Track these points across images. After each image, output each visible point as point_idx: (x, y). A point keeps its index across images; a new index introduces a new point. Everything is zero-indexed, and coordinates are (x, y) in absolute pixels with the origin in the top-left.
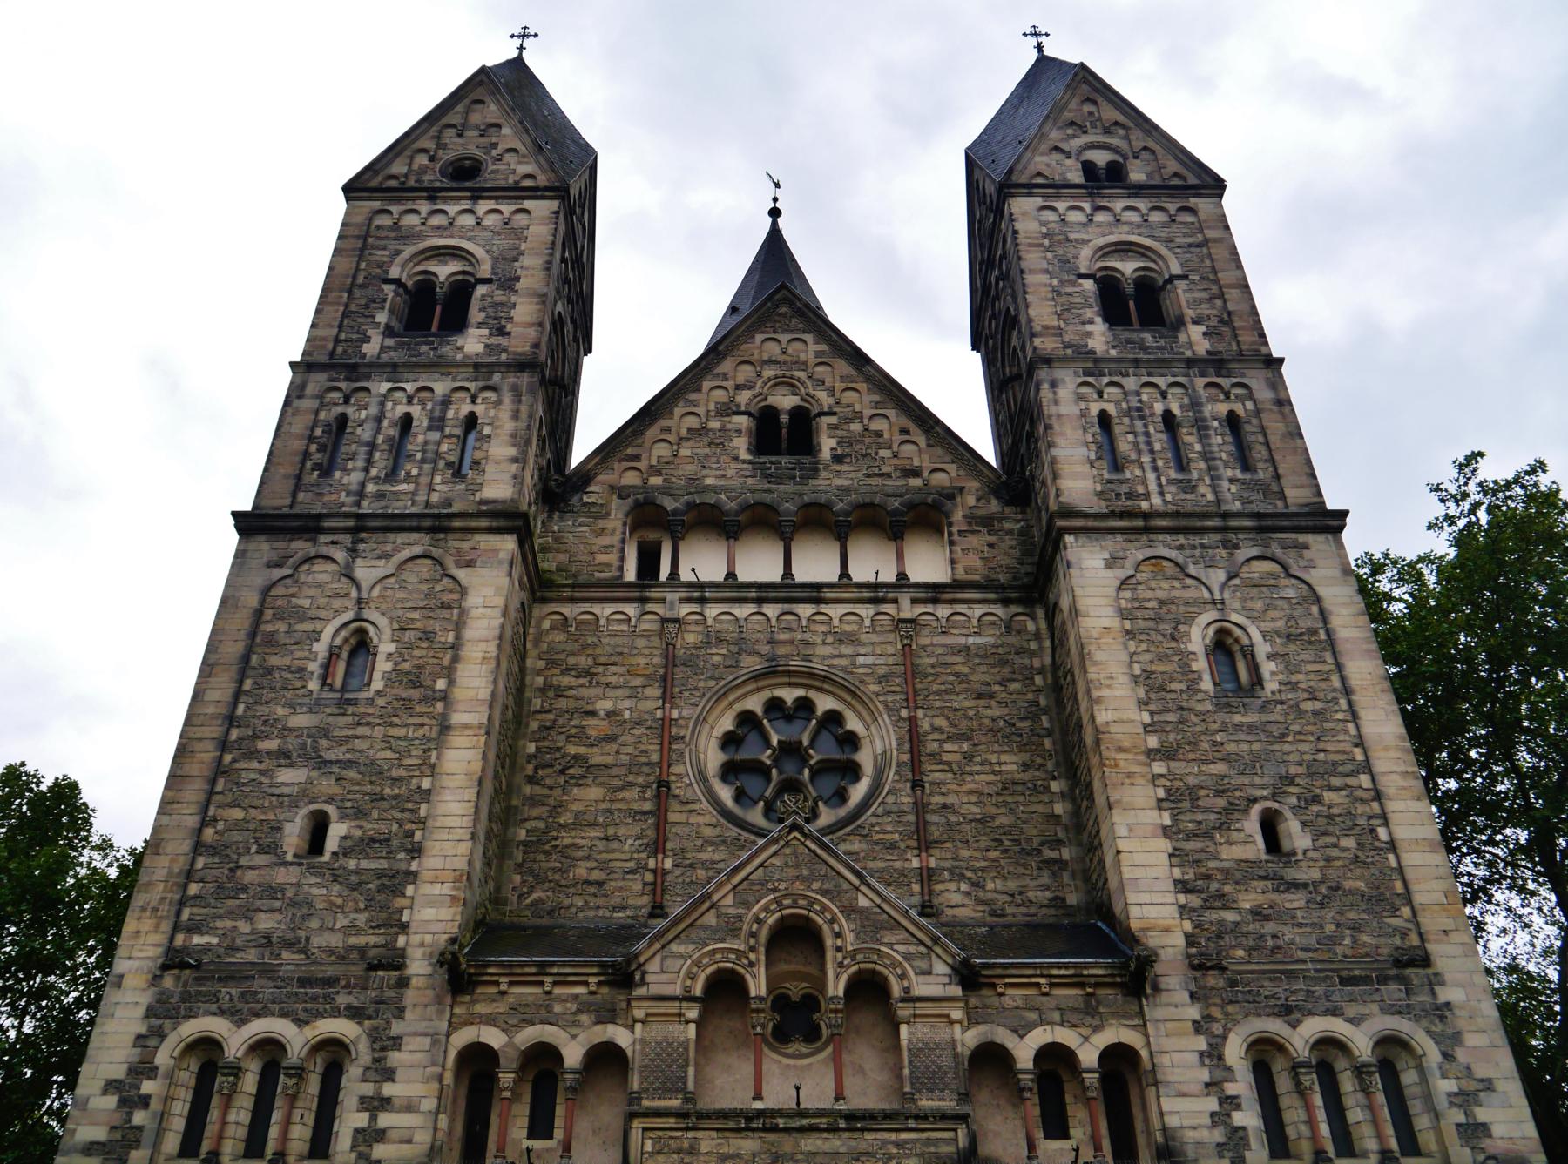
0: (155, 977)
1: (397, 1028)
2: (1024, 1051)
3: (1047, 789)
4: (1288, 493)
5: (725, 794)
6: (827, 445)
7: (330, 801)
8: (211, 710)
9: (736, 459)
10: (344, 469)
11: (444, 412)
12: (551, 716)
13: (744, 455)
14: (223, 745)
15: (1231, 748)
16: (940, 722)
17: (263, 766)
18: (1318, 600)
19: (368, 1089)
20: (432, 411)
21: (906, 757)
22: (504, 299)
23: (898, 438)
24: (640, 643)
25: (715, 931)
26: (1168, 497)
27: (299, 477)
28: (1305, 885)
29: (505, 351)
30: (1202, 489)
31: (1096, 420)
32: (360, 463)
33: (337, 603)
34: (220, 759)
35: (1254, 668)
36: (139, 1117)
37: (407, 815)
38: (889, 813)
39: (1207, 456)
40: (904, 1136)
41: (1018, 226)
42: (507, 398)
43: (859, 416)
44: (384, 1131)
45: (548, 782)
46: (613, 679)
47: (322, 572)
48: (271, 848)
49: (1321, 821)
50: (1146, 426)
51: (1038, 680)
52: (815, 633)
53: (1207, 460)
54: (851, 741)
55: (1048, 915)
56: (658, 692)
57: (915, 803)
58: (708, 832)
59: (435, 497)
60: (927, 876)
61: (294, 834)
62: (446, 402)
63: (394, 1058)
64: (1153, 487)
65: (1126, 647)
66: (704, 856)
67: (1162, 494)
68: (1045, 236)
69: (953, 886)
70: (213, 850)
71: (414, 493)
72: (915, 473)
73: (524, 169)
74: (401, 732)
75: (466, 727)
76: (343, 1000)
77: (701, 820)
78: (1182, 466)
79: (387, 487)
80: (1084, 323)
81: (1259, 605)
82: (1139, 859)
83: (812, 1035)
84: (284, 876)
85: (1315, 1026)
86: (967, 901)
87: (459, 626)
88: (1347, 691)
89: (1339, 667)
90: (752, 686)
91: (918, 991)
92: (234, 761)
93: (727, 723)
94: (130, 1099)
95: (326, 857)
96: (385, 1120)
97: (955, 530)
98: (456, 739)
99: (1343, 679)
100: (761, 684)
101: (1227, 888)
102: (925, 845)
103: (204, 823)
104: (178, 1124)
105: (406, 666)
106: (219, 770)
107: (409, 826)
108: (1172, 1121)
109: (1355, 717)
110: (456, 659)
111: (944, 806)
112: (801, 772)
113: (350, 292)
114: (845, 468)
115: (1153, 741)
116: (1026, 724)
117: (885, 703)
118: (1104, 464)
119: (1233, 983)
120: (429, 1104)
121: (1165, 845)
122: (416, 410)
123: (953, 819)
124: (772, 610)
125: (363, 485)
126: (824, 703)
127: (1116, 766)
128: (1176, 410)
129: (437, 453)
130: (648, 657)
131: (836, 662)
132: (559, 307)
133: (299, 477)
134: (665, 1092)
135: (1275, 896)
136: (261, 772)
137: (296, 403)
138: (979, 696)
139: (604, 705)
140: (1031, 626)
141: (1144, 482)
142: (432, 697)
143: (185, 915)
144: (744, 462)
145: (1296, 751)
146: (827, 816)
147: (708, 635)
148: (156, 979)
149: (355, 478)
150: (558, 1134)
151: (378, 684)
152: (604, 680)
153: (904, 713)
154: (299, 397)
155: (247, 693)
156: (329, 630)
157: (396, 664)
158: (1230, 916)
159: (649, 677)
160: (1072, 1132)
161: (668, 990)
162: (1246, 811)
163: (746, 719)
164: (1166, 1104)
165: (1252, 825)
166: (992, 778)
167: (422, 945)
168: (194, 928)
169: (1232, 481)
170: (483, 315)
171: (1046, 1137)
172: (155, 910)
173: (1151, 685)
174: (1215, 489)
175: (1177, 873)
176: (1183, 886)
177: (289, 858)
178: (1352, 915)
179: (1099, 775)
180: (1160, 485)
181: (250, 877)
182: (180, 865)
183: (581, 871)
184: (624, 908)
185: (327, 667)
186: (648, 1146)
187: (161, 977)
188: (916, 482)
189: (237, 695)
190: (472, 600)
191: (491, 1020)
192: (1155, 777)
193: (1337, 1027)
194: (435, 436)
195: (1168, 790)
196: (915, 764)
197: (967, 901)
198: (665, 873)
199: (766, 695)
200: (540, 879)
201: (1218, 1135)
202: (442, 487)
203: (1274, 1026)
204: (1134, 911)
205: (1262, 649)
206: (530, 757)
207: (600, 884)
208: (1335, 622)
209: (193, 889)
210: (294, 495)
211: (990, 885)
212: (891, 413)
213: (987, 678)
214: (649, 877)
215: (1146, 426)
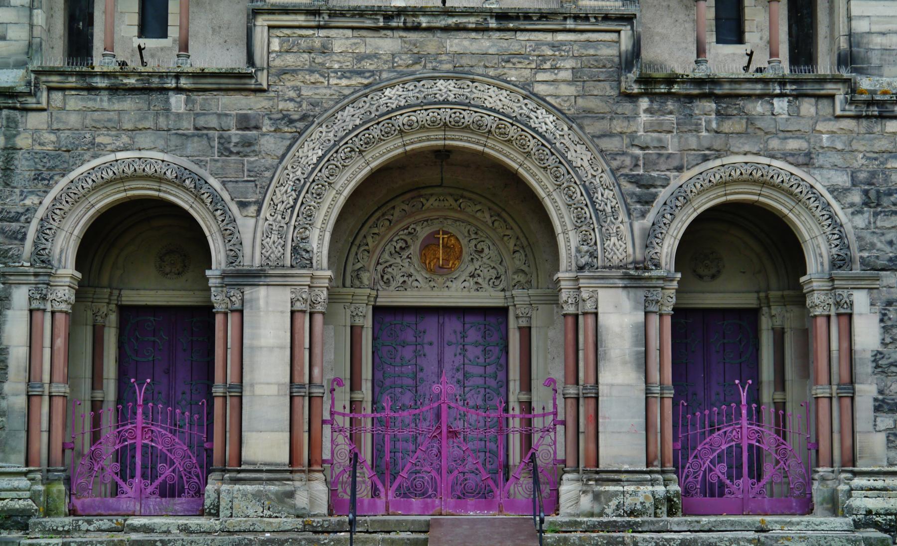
40: (561, 37)
108: (860, 26)
150: (173, 32)
160: (747, 36)
171: (718, 42)
186: (275, 45)
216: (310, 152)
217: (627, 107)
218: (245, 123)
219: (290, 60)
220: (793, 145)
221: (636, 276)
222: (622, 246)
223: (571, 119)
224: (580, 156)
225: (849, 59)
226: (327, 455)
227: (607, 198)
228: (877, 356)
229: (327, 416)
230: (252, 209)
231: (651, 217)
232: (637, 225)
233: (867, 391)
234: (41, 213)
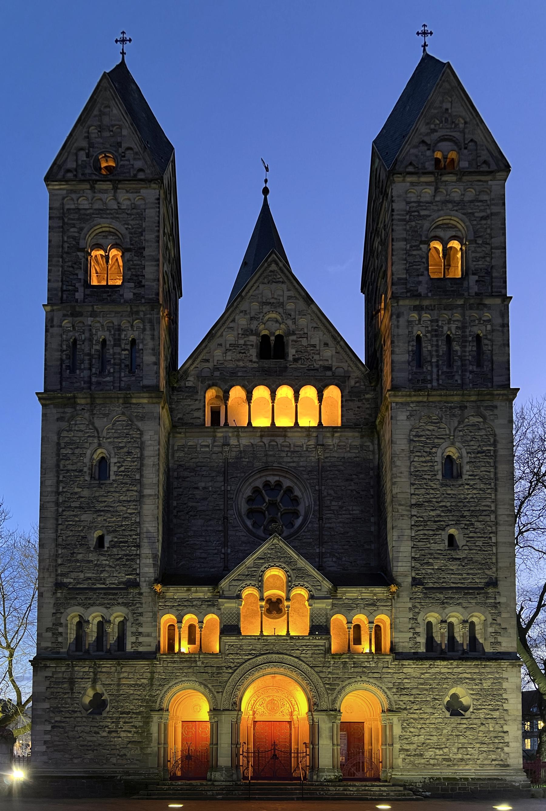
0: (54, 593)
1: (140, 610)
4: (495, 379)
5: (249, 523)
8: (49, 489)
10: (80, 369)
11: (120, 335)
14: (57, 504)
16: (331, 492)
17: (74, 513)
19: (134, 629)
20: (114, 335)
21: (317, 508)
22: (139, 262)
25: (248, 575)
27: (61, 373)
29: (143, 297)
31: (415, 338)
32: (86, 364)
34: (57, 510)
36: (60, 639)
37: (132, 533)
38: (309, 531)
41: (395, 206)
42: (148, 327)
44: (141, 643)
46: (204, 473)
51: (371, 472)
53: (462, 361)
54: (296, 501)
56: (222, 479)
57: (319, 527)
58: (243, 539)
59: (123, 384)
65: (410, 459)
66: (241, 548)
68: (408, 212)
69: (330, 559)
71: (113, 382)
73: (139, 164)
74: (125, 499)
76: (120, 601)
77: (240, 534)
78: (450, 365)
79: (100, 379)
80: (418, 275)
86: (335, 565)
90: (259, 475)
92: (63, 511)
93: (248, 492)
95: (106, 549)
96: (141, 639)
98: (147, 501)
100: (262, 474)
105: (122, 469)
107: (134, 537)
110: (142, 465)
111: (330, 528)
112: (277, 514)
117: (310, 484)
118: (414, 363)
123: (332, 533)
125: (90, 377)
127: (398, 511)
129: (121, 360)
131: (291, 465)
132: (165, 269)
133: (61, 373)
136: (75, 516)
137: (51, 330)
138: (347, 480)
140: (371, 448)
143: (59, 572)
149: (86, 373)
152: (200, 473)
153: (317, 488)
154: (52, 327)
155: (62, 481)
163: (256, 490)
167: (145, 581)
168: (63, 575)
172: (48, 569)
177: (92, 549)
179: (391, 515)
181: (80, 557)
187: (56, 593)
190: (146, 437)
194: (117, 350)
197: (335, 565)
198: (228, 554)
199: (264, 479)
206: (175, 507)
209: (60, 561)
210: (61, 384)
211: (344, 559)
214: (222, 556)
215: (437, 341)
223: (311, 667)
226: (241, 764)
227: (322, 690)
229: (241, 753)
230: (221, 693)
231: (334, 695)
232: (330, 698)
234: (161, 696)
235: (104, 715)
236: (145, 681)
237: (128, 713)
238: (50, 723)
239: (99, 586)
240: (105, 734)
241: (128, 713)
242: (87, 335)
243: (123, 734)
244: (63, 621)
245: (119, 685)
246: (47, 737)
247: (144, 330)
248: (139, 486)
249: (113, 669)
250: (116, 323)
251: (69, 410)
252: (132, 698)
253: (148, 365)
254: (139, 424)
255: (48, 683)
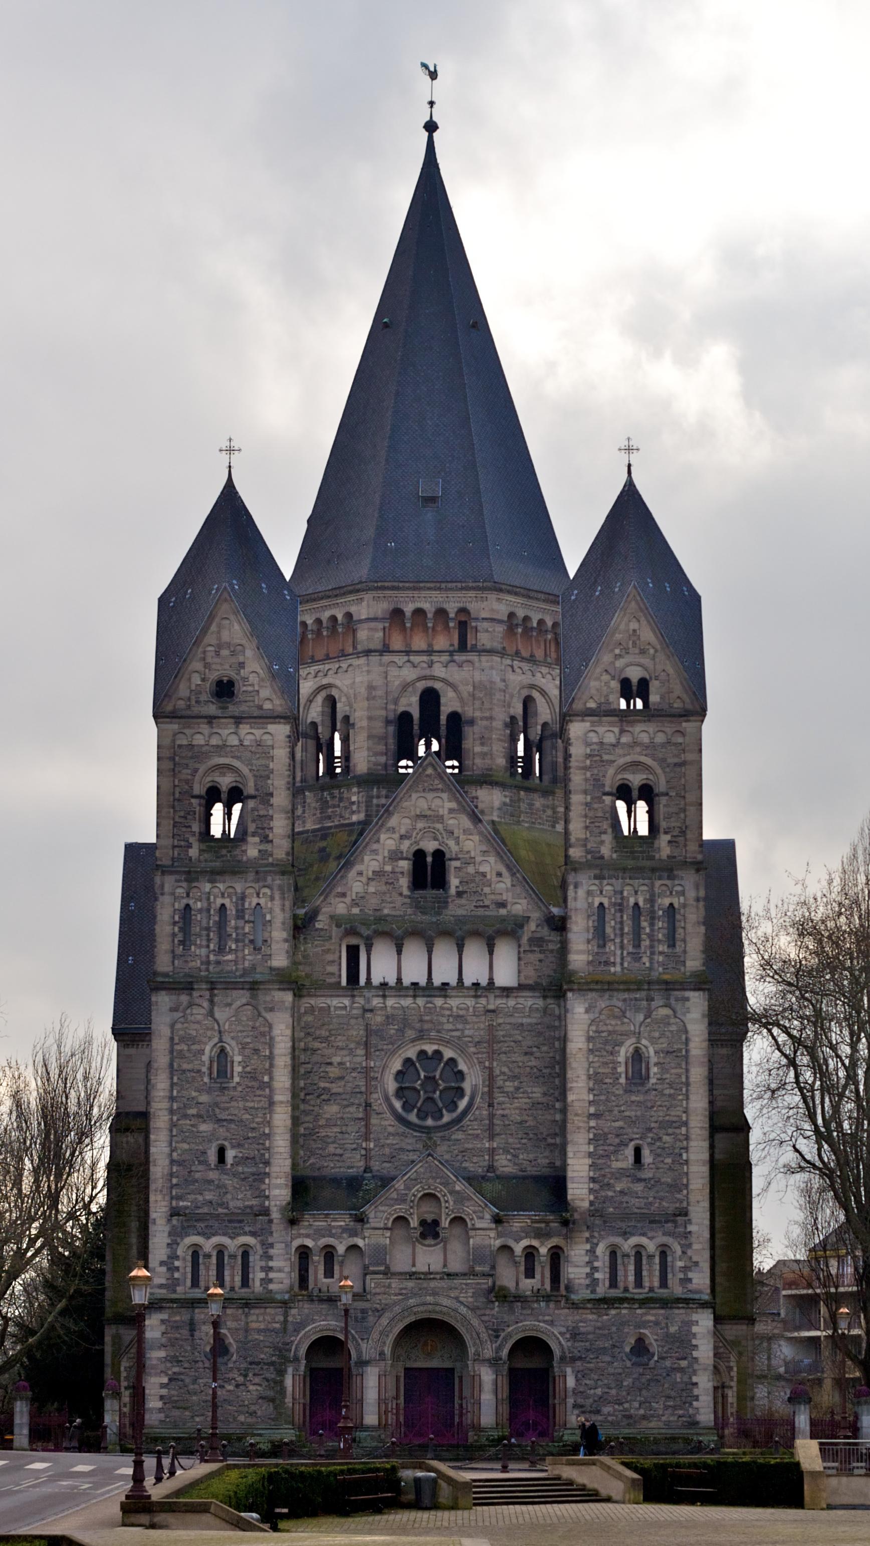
1: (270, 1240)
2: (518, 1248)
3: (554, 1106)
6: (454, 882)
7: (225, 1139)
8: (162, 1094)
9: (401, 894)
11: (243, 905)
12: (309, 1066)
13: (406, 892)
14: (171, 1112)
15: (627, 1114)
18: (686, 1032)
19: (263, 1264)
23: (495, 879)
24: (353, 1021)
26: (626, 965)
27: (173, 952)
28: (645, 1180)
30: (645, 960)
32: (204, 943)
33: (209, 1033)
34: (172, 1119)
35: (648, 1069)
36: (176, 1275)
39: (651, 936)
43: (471, 861)
45: (312, 1102)
47: (198, 1013)
48: (205, 1163)
49: (659, 1151)
50: (622, 917)
52: (443, 1016)
55: (546, 1171)
60: (492, 1152)
61: (212, 1157)
62: (243, 898)
63: (272, 1252)
64: (618, 960)
67: (622, 964)
70: (180, 1163)
72: (503, 905)
74: (251, 1104)
75: (282, 1102)
76: (247, 1229)
81: (657, 1034)
82: (575, 1168)
83: (436, 1235)
84: (213, 1175)
85: (634, 1240)
87: (271, 1046)
88: (687, 1084)
89: (687, 1071)
91: (478, 1225)
94: (172, 1269)
96: (272, 1275)
97: (522, 950)
98: (278, 1109)
99: (687, 1078)
101: (612, 1181)
102: (492, 1137)
103: (172, 1151)
104: (189, 1276)
105: (248, 1069)
106: (173, 1125)
108: (572, 1276)
109: (687, 1099)
110: (272, 1065)
113: (173, 807)
114: (463, 901)
115: (592, 1110)
116: (547, 1071)
119: (605, 1222)
120: (287, 1269)
121: (588, 1161)
122: (227, 902)
124: (421, 1001)
125: (208, 957)
126: (448, 1054)
128: (641, 904)
130: (357, 1032)
133: (173, 952)
134: (378, 1264)
135: (631, 1185)
139: (336, 1060)
141: (615, 955)
142: (263, 1086)
144: (406, 897)
145: (658, 1114)
146: (447, 1118)
147: (387, 1017)
148: (169, 1221)
149: (204, 951)
151: (237, 1079)
155: (176, 1084)
156: (208, 1049)
157: (244, 1068)
158: (610, 1194)
159: (358, 1043)
161: (377, 1225)
162: (627, 1145)
164: (570, 1270)
165: (629, 1152)
166: (527, 1100)
168: (179, 1198)
169: (660, 953)
170: (254, 825)
173: (596, 1079)
174: (651, 960)
175: (592, 1174)
176: (593, 1180)
178: (661, 1194)
180: (622, 959)
181: (197, 1175)
182: (166, 1171)
183: (331, 1149)
184: (352, 1167)
185: (210, 1068)
188: (503, 912)
189: (172, 1085)
190: (276, 1032)
191: (307, 1236)
192: (590, 1128)
193: (644, 1240)
194: (241, 923)
195: (595, 1135)
196: (490, 1093)
200: (313, 1154)
201: (588, 1282)
202: (249, 957)
203: (618, 1240)
204: (570, 1192)
205: (653, 1059)
207: (341, 1155)
208: (692, 1045)
209: (175, 1181)
212: (492, 859)
213: (530, 1043)
216: (384, 1321)
217: (491, 1306)
218: (364, 1311)
219: (378, 1290)
220: (547, 1318)
221: (494, 1362)
222: (488, 1353)
224: (475, 1322)
225: (568, 1288)
228: (574, 1389)
233: (570, 1401)
235: (230, 1365)
236: (277, 1326)
237: (258, 1363)
238: (167, 1375)
239: (220, 1210)
240: (231, 1388)
241: (258, 1363)
242: (205, 905)
243: (251, 1388)
244: (179, 1252)
245: (246, 1331)
246: (164, 1392)
247: (272, 898)
248: (267, 1090)
249: (240, 1311)
250: (239, 891)
251: (184, 998)
252: (262, 1345)
253: (277, 942)
254: (268, 1016)
255: (164, 1327)
